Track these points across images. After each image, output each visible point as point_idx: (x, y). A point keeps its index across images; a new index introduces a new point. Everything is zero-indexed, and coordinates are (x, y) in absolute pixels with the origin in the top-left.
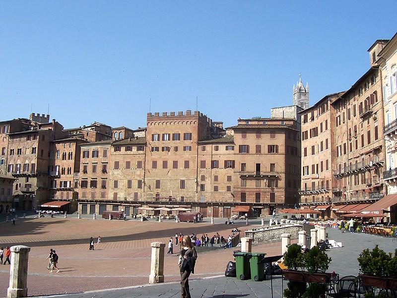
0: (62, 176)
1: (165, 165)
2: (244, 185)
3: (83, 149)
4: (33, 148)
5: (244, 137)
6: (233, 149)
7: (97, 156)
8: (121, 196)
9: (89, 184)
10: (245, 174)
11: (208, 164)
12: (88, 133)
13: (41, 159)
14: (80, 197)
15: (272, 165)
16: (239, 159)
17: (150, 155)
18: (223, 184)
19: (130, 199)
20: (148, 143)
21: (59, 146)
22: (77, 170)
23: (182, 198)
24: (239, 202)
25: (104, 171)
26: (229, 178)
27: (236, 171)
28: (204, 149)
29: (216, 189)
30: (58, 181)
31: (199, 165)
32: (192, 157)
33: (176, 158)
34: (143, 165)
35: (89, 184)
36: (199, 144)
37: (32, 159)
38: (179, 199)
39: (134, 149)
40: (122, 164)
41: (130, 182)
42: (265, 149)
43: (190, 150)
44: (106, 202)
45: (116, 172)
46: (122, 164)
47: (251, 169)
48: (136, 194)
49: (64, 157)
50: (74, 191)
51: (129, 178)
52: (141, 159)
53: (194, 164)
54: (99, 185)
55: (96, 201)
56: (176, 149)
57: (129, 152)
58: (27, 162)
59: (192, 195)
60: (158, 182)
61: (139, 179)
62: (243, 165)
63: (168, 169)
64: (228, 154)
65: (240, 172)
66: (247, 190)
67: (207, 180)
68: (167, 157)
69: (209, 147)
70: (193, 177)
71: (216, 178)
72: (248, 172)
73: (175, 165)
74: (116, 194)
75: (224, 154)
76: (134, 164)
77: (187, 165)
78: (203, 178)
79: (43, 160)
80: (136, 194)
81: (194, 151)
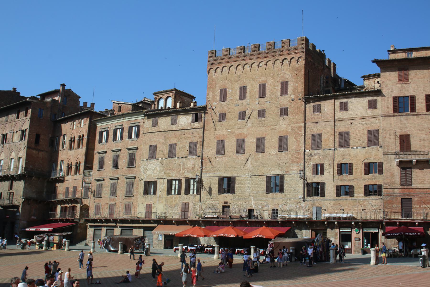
0: (67, 178)
1: (241, 146)
2: (406, 180)
3: (100, 126)
4: (23, 131)
5: (403, 79)
10: (408, 157)
11: (328, 139)
12: (120, 107)
13: (34, 149)
14: (92, 214)
17: (213, 130)
18: (358, 180)
20: (209, 107)
21: (66, 127)
22: (89, 166)
23: (275, 212)
25: (131, 162)
27: (387, 150)
28: (317, 110)
30: (61, 188)
31: (309, 142)
32: (293, 128)
33: (260, 132)
34: (199, 149)
36: (307, 101)
37: (20, 149)
40: (163, 150)
44: (133, 221)
46: (163, 150)
48: (185, 206)
50: (82, 203)
53: (298, 142)
55: (116, 221)
56: (262, 114)
57: (174, 127)
59: (294, 205)
61: (190, 176)
62: (405, 142)
63: (246, 155)
65: (396, 154)
66: (416, 192)
67: (326, 173)
68: (245, 131)
69: (327, 106)
72: (417, 153)
73: (261, 145)
74: (149, 207)
77: (283, 144)
79: (40, 151)
80: (185, 206)
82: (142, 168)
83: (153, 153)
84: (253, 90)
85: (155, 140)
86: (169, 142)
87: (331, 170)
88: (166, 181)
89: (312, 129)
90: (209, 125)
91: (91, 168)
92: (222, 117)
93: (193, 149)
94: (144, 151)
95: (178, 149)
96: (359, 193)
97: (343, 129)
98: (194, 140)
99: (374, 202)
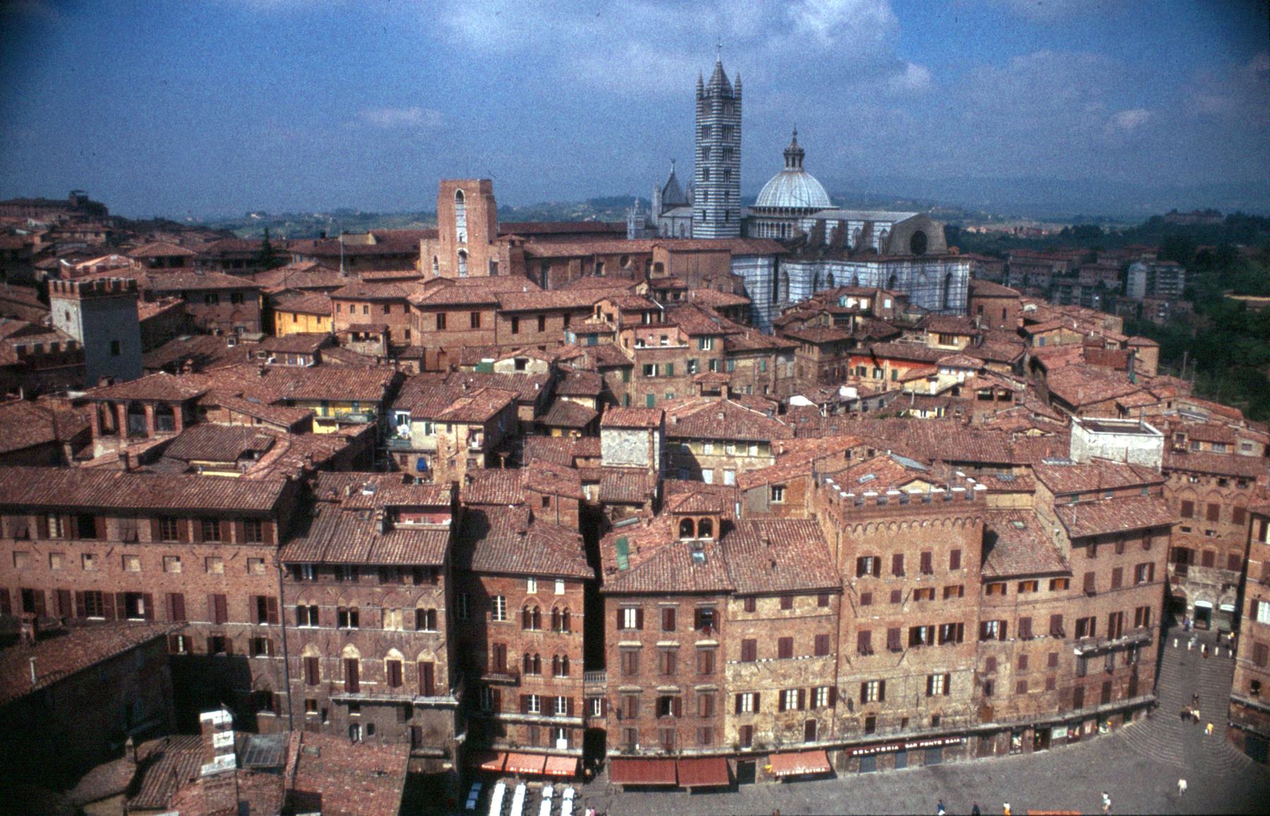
5: (1092, 554)
6: (1066, 586)
26: (1053, 660)
29: (1021, 688)
34: (832, 645)
43: (961, 594)
45: (747, 670)
49: (530, 619)
52: (827, 628)
54: (691, 708)
57: (787, 613)
58: (394, 654)
61: (818, 682)
64: (1056, 600)
67: (1001, 669)
71: (1023, 662)
75: (1045, 601)
76: (804, 641)
78: (992, 664)
81: (970, 598)
82: (729, 674)
83: (749, 652)
84: (912, 560)
85: (751, 633)
86: (778, 635)
87: (1008, 665)
88: (776, 693)
90: (847, 612)
93: (821, 647)
94: (734, 648)
95: (795, 645)
97: (1024, 615)
98: (823, 632)
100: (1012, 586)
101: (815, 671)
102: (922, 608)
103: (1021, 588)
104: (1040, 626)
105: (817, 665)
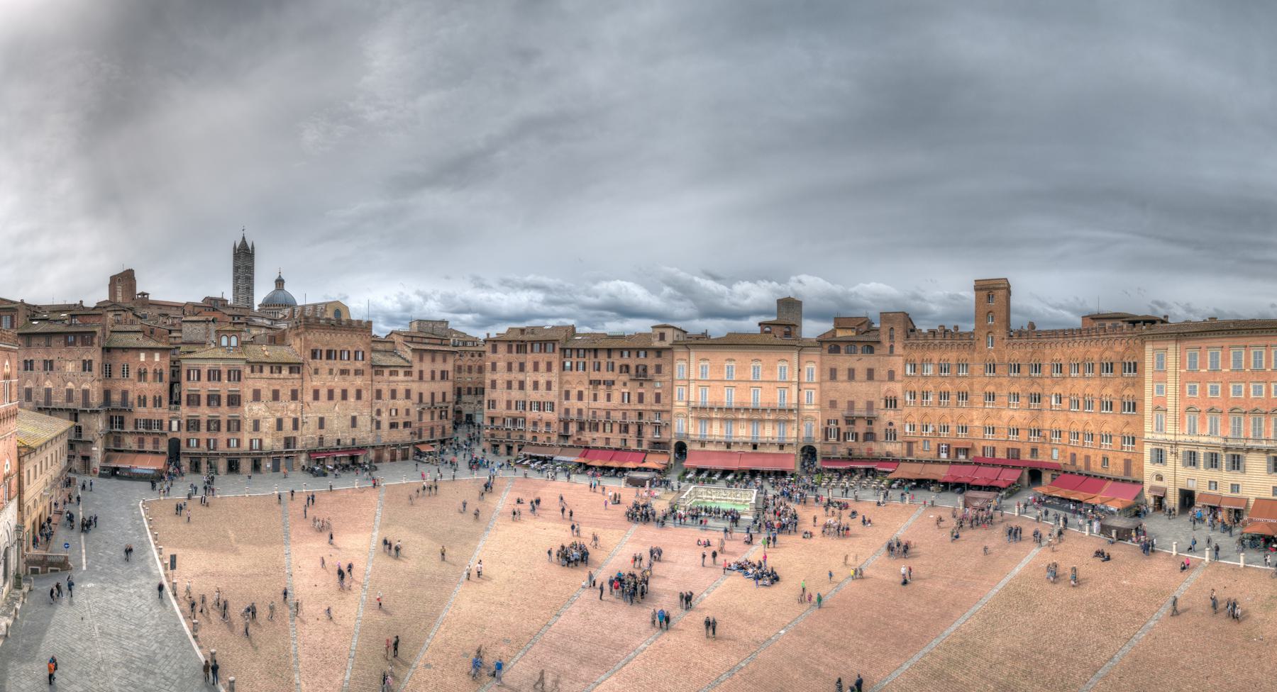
2: (420, 419)
5: (421, 360)
7: (219, 380)
8: (268, 443)
9: (203, 426)
11: (386, 394)
15: (444, 394)
16: (415, 388)
19: (280, 446)
24: (416, 440)
26: (408, 412)
33: (345, 385)
35: (203, 426)
38: (349, 442)
39: (285, 372)
41: (280, 423)
42: (438, 376)
46: (266, 394)
47: (427, 399)
51: (278, 415)
57: (276, 375)
60: (322, 420)
62: (421, 395)
70: (366, 411)
73: (344, 395)
76: (285, 393)
78: (379, 412)
81: (367, 377)
83: (257, 396)
85: (260, 385)
89: (377, 386)
90: (307, 377)
91: (178, 403)
92: (316, 371)
96: (401, 427)
99: (408, 431)
100: (386, 372)
101: (290, 409)
102: (344, 380)
103: (391, 374)
104: (401, 393)
105: (293, 406)
